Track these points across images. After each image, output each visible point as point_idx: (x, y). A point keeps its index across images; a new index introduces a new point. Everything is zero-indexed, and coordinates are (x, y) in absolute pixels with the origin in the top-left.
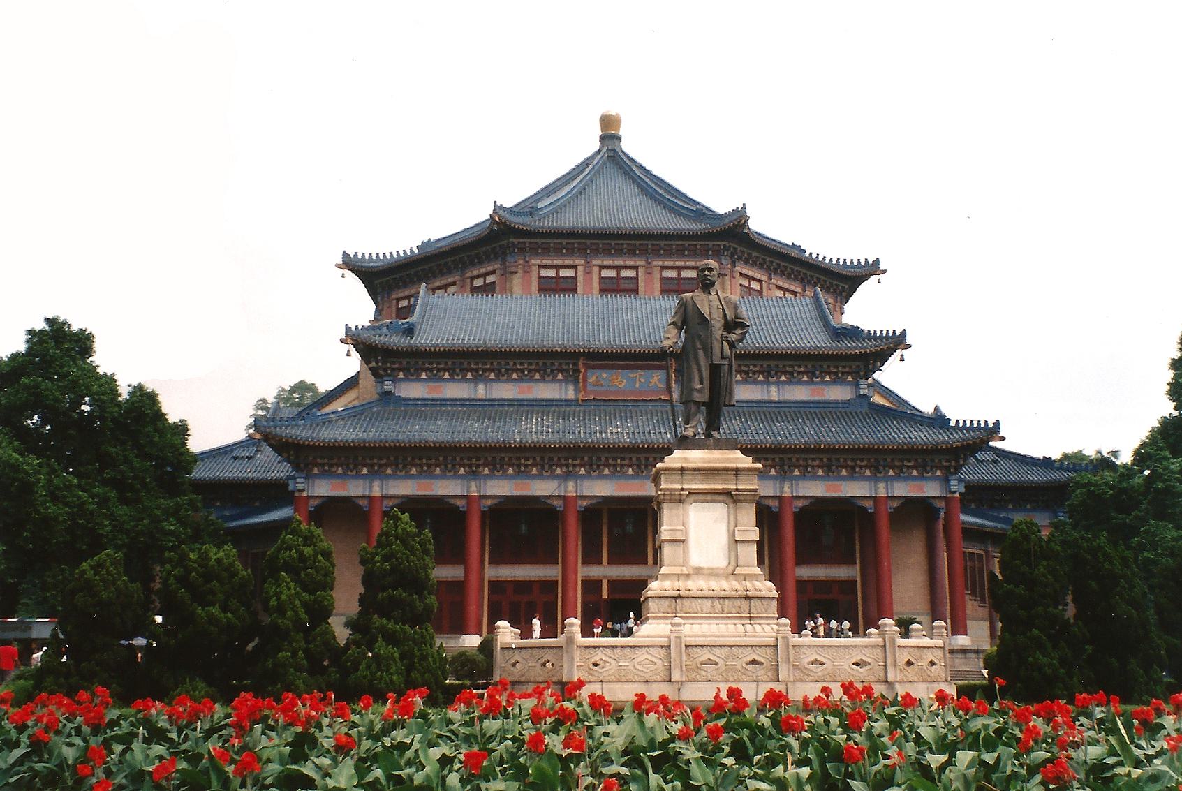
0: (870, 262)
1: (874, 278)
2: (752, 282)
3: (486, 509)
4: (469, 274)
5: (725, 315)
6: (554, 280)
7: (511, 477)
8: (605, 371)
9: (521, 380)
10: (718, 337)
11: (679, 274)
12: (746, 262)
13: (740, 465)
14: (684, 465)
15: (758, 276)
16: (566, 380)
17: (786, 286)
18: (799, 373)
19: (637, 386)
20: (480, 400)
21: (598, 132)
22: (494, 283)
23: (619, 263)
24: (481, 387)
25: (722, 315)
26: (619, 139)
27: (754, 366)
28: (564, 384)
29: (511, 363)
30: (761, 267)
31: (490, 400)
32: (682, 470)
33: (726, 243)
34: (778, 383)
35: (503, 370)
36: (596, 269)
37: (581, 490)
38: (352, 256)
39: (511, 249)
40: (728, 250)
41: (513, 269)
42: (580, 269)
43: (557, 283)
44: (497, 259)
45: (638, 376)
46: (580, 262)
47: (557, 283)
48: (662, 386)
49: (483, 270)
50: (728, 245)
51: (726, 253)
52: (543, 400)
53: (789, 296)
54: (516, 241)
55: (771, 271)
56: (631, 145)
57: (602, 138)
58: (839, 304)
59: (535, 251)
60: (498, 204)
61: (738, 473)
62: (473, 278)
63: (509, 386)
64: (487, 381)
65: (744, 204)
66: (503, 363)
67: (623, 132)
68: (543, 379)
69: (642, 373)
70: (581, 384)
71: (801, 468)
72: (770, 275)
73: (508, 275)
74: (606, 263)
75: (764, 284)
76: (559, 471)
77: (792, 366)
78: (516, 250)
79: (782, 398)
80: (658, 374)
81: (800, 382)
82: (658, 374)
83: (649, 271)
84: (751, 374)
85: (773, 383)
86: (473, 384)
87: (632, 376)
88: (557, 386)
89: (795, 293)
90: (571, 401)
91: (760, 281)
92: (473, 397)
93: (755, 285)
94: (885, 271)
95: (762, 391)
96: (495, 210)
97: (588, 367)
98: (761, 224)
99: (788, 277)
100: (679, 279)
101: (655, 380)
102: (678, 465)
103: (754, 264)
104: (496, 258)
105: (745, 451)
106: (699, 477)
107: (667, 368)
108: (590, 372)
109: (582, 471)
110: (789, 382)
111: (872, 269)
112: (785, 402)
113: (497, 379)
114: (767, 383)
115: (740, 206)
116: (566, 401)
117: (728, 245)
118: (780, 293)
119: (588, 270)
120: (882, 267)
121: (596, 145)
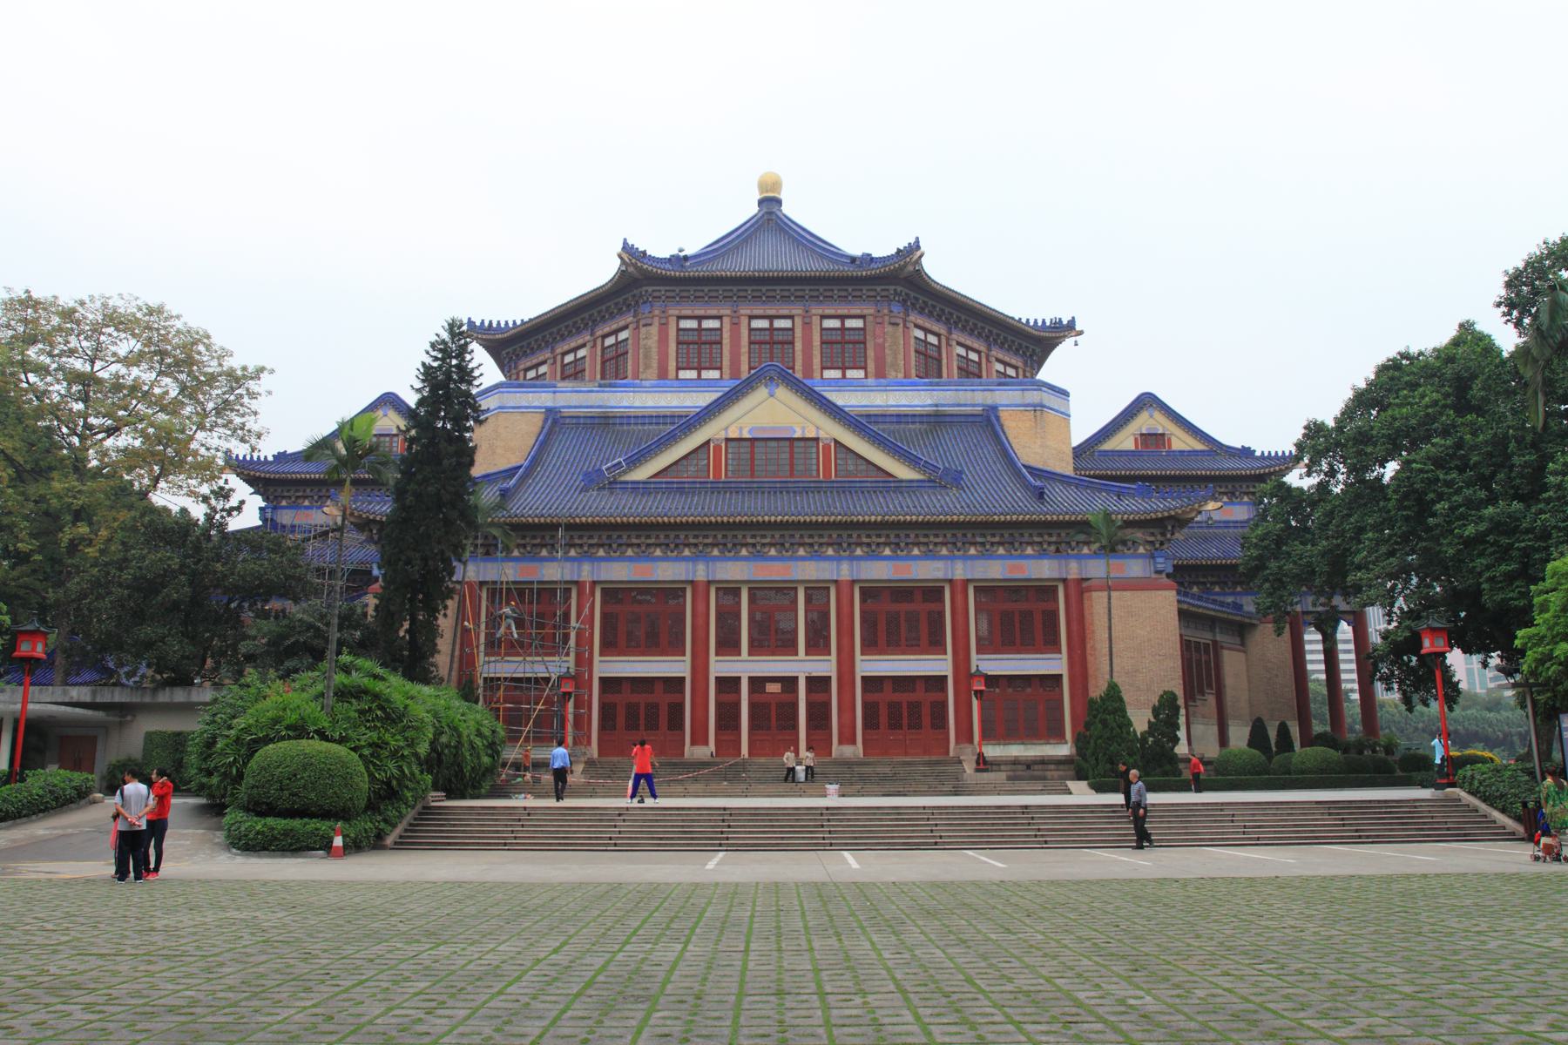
0: (1065, 322)
1: (1069, 342)
4: (599, 333)
11: (843, 324)
12: (921, 311)
21: (758, 197)
26: (779, 202)
30: (939, 319)
33: (899, 289)
38: (478, 324)
40: (900, 295)
41: (649, 321)
42: (726, 320)
43: (700, 336)
46: (726, 311)
47: (700, 336)
54: (650, 289)
55: (951, 324)
56: (792, 209)
57: (761, 202)
58: (1028, 369)
60: (630, 242)
65: (917, 238)
67: (783, 196)
74: (756, 312)
83: (807, 320)
94: (1081, 333)
96: (624, 248)
98: (941, 269)
103: (930, 315)
111: (1061, 331)
115: (912, 241)
120: (1078, 328)
121: (752, 209)
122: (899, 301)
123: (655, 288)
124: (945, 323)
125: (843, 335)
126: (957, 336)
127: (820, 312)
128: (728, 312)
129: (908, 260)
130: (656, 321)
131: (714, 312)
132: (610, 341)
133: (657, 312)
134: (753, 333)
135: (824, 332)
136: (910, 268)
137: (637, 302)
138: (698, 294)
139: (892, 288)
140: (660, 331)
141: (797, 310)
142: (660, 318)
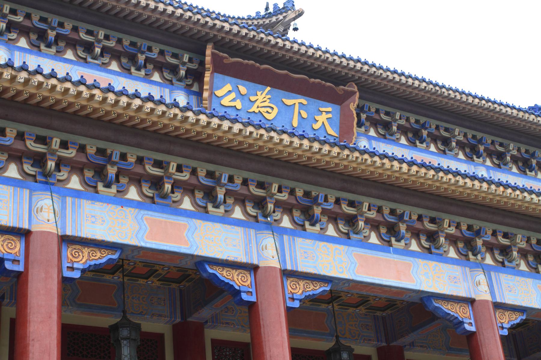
3: (76, 275)
8: (247, 83)
37: (294, 260)
45: (297, 107)
69: (304, 102)
80: (329, 109)
82: (329, 109)
101: (322, 118)
129: (281, 17)
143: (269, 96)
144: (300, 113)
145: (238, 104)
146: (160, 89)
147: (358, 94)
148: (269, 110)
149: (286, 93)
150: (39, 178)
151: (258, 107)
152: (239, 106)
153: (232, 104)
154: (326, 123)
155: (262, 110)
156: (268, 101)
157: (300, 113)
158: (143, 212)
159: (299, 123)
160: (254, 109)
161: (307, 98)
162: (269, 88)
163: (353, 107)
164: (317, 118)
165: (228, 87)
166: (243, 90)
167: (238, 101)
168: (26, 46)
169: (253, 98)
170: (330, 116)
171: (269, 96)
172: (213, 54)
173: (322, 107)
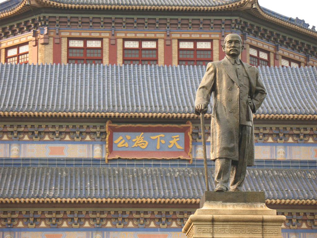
2: (261, 53)
4: (4, 45)
5: (250, 83)
6: (82, 51)
7: (43, 229)
9: (52, 141)
10: (245, 102)
11: (195, 45)
13: (266, 217)
14: (215, 216)
15: (266, 47)
16: (93, 142)
17: (291, 56)
18: (305, 135)
19: (158, 147)
20: (15, 160)
22: (27, 53)
23: (141, 35)
24: (15, 147)
25: (248, 83)
27: (265, 129)
28: (91, 145)
29: (44, 126)
30: (268, 39)
31: (23, 159)
32: (213, 221)
34: (286, 144)
35: (36, 133)
36: (120, 41)
39: (43, 23)
40: (240, 24)
42: (106, 41)
44: (30, 31)
46: (106, 35)
48: (180, 147)
49: (17, 42)
50: (239, 20)
51: (237, 27)
52: (71, 160)
53: (295, 65)
54: (47, 15)
55: (278, 42)
59: (63, 23)
61: (264, 224)
62: (7, 49)
63: (42, 146)
64: (20, 141)
66: (36, 126)
68: (73, 142)
70: (107, 146)
71: (308, 222)
72: (277, 46)
73: (40, 46)
74: (129, 35)
75: (272, 56)
76: (87, 224)
77: (298, 129)
78: (47, 24)
79: (288, 158)
80: (178, 136)
81: (306, 144)
82: (178, 136)
84: (261, 137)
85: (280, 144)
86: (8, 145)
87: (152, 137)
88: (85, 147)
89: (299, 63)
90: (98, 160)
91: (268, 52)
92: (8, 156)
93: (264, 56)
95: (272, 152)
97: (113, 130)
99: (293, 48)
100: (195, 50)
102: (209, 216)
103: (262, 36)
104: (29, 30)
105: (270, 206)
106: (228, 227)
107: (185, 130)
108: (115, 134)
109: (109, 224)
110: (296, 143)
112: (293, 162)
113: (31, 141)
114: (275, 143)
116: (94, 160)
117: (239, 20)
118: (285, 63)
119: (113, 42)
122: (238, 29)
123: (51, 15)
124: (274, 42)
125: (195, 55)
126: (282, 51)
127: (178, 36)
128: (108, 35)
130: (51, 43)
131: (97, 35)
132: (12, 52)
133: (52, 34)
134: (126, 52)
135: (181, 52)
136: (249, 6)
137: (36, 26)
138: (84, 20)
139: (234, 18)
140: (54, 49)
141: (160, 35)
142: (54, 38)
143: (143, 137)
144: (160, 142)
145: (126, 145)
146: (88, 146)
147: (191, 127)
148: (143, 144)
149: (153, 133)
150: (6, 226)
151: (137, 144)
152: (127, 146)
153: (123, 145)
154: (176, 144)
155: (139, 145)
156: (142, 139)
157: (160, 142)
158: (45, 233)
159: (161, 147)
160: (135, 145)
161: (164, 133)
162: (143, 133)
163: (189, 134)
164: (170, 142)
165: (121, 138)
166: (128, 137)
167: (126, 143)
168: (28, 139)
169: (134, 140)
170: (178, 139)
171: (143, 137)
172: (109, 126)
173: (173, 136)
